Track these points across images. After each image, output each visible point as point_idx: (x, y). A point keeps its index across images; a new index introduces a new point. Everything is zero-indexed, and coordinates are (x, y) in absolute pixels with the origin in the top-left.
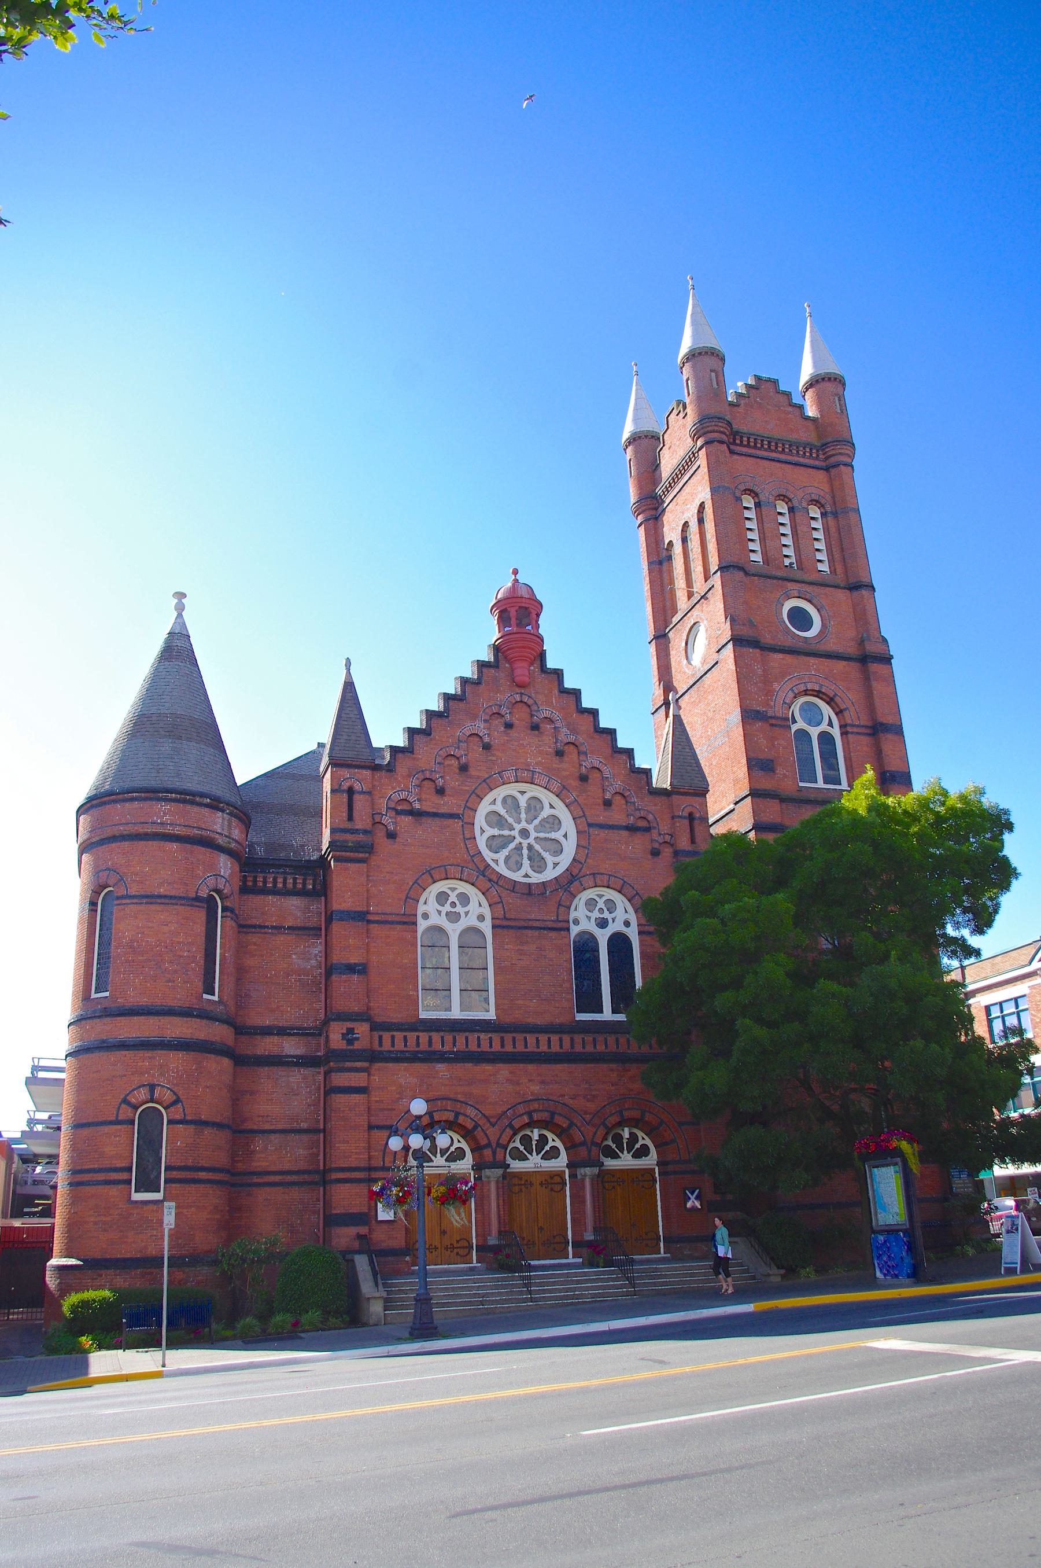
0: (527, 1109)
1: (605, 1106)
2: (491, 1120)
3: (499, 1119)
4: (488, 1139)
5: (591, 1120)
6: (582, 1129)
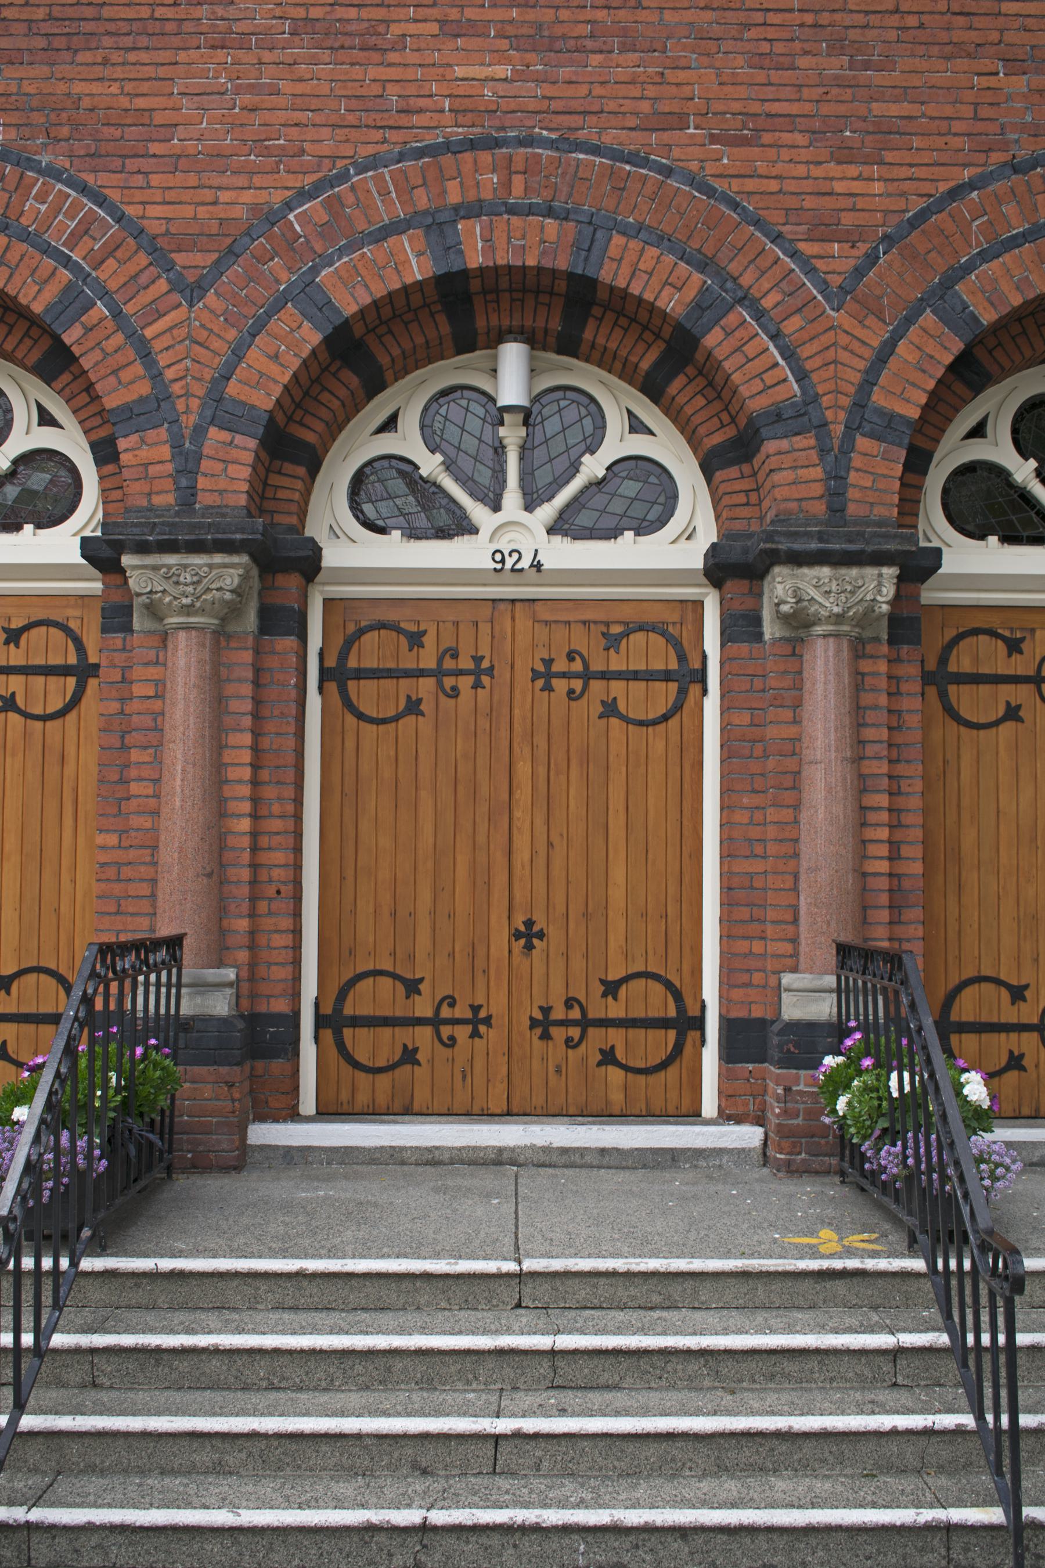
0: (422, 200)
1: (955, 193)
2: (180, 259)
3: (232, 253)
4: (156, 376)
5: (859, 273)
6: (792, 326)
